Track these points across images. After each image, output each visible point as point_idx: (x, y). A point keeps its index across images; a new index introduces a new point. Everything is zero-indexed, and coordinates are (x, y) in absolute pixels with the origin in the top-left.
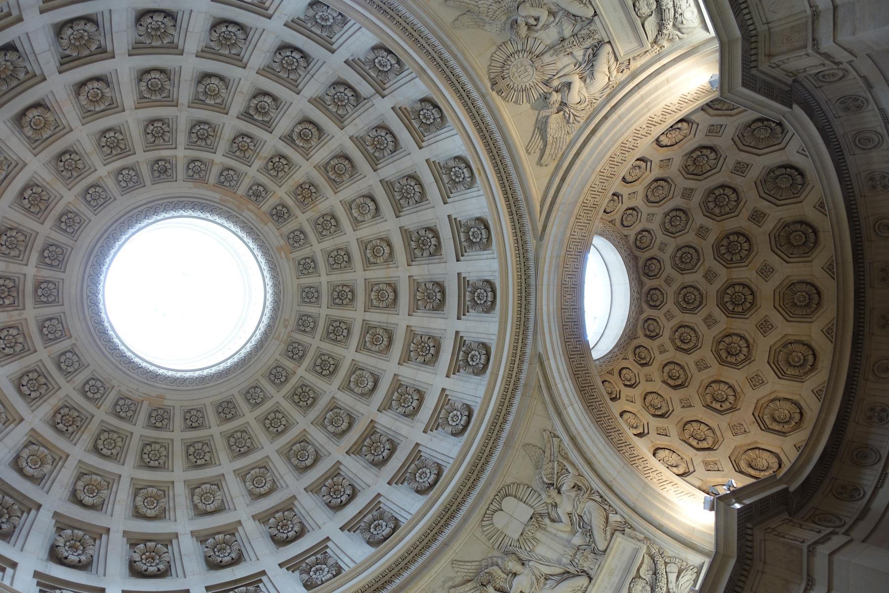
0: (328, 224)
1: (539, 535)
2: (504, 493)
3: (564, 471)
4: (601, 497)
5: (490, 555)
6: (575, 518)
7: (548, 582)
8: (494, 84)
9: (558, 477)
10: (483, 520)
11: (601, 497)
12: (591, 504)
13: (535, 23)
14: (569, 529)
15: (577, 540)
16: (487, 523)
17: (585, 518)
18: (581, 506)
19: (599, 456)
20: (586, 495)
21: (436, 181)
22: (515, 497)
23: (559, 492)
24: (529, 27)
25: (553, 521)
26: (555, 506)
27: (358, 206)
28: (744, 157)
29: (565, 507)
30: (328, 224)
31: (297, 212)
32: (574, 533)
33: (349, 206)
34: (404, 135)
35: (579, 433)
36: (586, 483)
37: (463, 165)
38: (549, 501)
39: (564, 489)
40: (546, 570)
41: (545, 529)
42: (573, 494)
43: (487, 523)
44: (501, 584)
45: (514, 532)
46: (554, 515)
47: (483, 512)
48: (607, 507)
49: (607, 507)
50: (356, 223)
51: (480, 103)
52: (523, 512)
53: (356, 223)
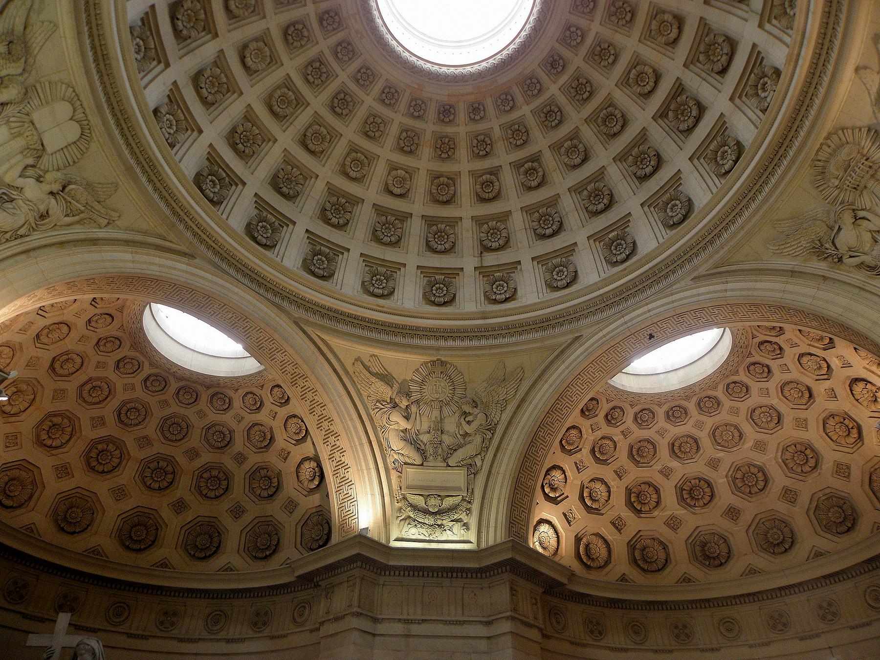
0: (408, 143)
8: (443, 363)
13: (467, 419)
21: (383, 260)
24: (465, 414)
27: (404, 179)
28: (247, 518)
30: (408, 143)
31: (437, 128)
33: (410, 173)
34: (436, 261)
37: (386, 293)
50: (393, 167)
51: (432, 343)
53: (393, 167)
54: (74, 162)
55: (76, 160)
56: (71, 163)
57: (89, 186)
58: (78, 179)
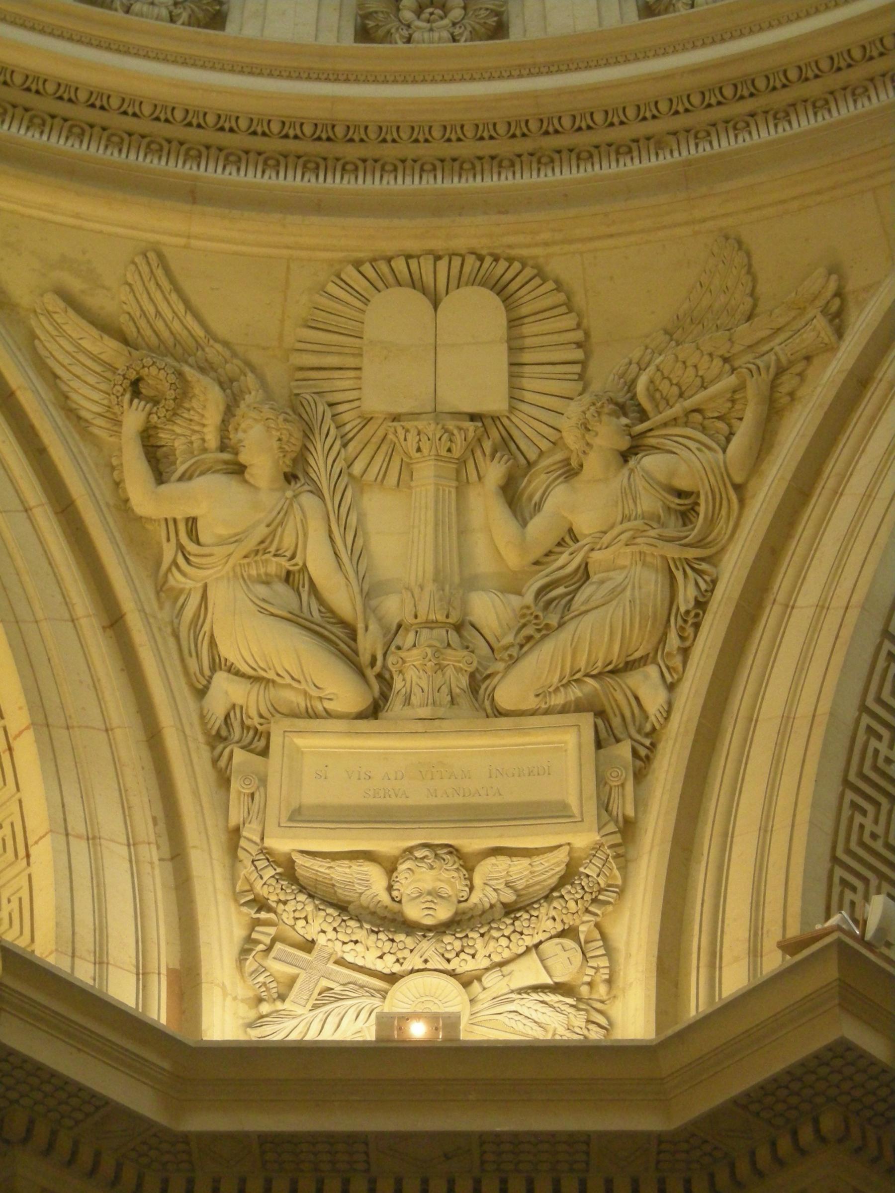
1: (426, 473)
2: (504, 280)
3: (714, 424)
5: (256, 357)
6: (567, 562)
7: (281, 588)
9: (674, 422)
10: (357, 264)
11: (701, 605)
12: (652, 584)
14: (513, 559)
15: (489, 610)
16: (360, 284)
17: (587, 591)
20: (672, 551)
22: (514, 322)
23: (625, 456)
25: (510, 492)
26: (570, 471)
32: (511, 585)
36: (722, 527)
38: (571, 439)
39: (650, 462)
40: (319, 562)
42: (649, 502)
43: (360, 284)
44: (179, 445)
45: (384, 386)
46: (535, 484)
47: (388, 246)
48: (673, 641)
49: (673, 641)
52: (476, 379)
54: (579, 345)
55: (579, 335)
56: (579, 355)
58: (636, 354)
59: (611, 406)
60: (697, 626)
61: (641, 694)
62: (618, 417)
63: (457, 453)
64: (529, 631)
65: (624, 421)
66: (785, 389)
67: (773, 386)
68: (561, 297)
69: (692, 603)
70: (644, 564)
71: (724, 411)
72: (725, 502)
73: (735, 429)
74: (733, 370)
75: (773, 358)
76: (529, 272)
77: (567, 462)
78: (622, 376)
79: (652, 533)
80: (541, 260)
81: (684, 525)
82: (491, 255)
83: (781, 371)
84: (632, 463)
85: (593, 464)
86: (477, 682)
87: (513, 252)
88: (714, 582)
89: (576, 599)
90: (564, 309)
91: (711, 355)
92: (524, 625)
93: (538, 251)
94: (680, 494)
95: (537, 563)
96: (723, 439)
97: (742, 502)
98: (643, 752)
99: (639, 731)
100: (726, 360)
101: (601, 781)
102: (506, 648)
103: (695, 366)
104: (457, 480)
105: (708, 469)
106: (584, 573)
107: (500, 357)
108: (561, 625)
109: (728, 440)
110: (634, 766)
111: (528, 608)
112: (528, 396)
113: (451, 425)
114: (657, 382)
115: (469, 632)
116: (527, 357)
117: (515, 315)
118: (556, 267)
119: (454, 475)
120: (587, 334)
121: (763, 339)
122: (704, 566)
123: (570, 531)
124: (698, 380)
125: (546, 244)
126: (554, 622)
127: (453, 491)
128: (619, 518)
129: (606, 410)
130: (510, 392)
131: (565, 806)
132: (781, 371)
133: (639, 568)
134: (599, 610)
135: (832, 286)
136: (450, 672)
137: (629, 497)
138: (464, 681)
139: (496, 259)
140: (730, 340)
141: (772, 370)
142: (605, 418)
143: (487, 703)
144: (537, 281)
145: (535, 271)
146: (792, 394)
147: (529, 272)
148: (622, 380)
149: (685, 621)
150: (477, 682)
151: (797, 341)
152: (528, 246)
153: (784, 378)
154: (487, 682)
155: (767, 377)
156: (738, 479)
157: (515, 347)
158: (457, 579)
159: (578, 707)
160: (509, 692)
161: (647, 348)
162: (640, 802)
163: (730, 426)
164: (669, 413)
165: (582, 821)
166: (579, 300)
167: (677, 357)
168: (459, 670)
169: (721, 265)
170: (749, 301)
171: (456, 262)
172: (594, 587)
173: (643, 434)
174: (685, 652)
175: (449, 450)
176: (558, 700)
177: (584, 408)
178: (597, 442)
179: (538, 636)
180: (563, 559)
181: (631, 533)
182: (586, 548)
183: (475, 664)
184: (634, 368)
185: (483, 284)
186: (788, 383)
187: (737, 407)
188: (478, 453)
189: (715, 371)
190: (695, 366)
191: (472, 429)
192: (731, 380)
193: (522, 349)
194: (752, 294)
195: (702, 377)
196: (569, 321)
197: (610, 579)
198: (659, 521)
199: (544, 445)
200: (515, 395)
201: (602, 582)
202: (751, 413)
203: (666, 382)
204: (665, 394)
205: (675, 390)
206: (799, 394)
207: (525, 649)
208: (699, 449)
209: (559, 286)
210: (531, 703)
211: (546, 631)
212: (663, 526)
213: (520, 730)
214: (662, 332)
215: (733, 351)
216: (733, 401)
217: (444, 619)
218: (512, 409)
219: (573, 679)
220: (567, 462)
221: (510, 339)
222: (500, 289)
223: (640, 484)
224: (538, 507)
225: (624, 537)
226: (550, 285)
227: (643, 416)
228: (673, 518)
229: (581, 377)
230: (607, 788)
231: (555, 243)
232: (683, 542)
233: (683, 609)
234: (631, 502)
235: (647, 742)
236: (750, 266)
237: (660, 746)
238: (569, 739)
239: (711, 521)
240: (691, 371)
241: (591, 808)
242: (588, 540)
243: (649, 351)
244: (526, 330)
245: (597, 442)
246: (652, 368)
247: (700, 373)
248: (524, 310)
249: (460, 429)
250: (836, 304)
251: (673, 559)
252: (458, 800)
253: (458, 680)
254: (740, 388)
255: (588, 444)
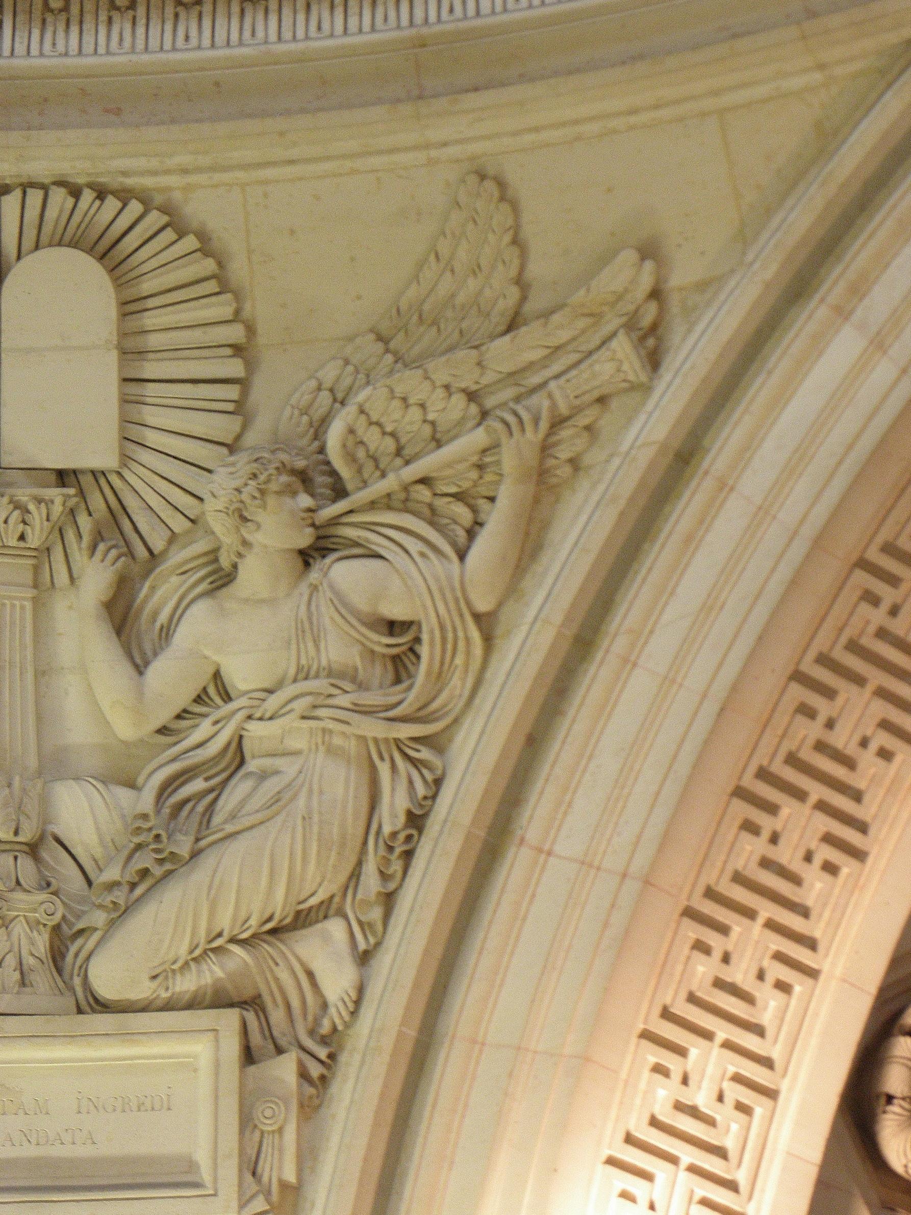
4: (416, 821)
6: (209, 735)
9: (386, 502)
11: (416, 821)
12: (339, 785)
14: (125, 728)
15: (85, 816)
17: (238, 790)
18: (296, 734)
19: (640, 686)
20: (374, 728)
22: (130, 307)
23: (306, 558)
25: (121, 614)
29: (240, 638)
35: (724, 487)
36: (458, 685)
38: (221, 526)
39: (344, 574)
41: (41, 589)
42: (339, 648)
46: (161, 594)
48: (371, 883)
49: (371, 883)
54: (238, 350)
55: (236, 333)
56: (235, 368)
57: (396, 340)
58: (329, 374)
59: (284, 478)
60: (408, 855)
61: (317, 967)
62: (294, 494)
63: (35, 539)
64: (144, 860)
65: (305, 500)
66: (564, 453)
67: (545, 449)
68: (209, 266)
69: (402, 819)
70: (331, 751)
71: (466, 485)
72: (461, 644)
73: (482, 517)
74: (484, 414)
75: (546, 404)
76: (155, 219)
77: (213, 555)
78: (305, 412)
79: (344, 700)
80: (177, 196)
81: (398, 681)
82: (90, 186)
83: (558, 422)
84: (314, 575)
85: (254, 575)
86: (63, 947)
87: (130, 182)
88: (438, 782)
89: (221, 802)
90: (211, 286)
91: (447, 387)
92: (139, 847)
93: (173, 180)
94: (392, 627)
95: (163, 731)
96: (461, 535)
97: (488, 640)
98: (315, 1070)
99: (312, 1033)
100: (472, 396)
101: (246, 1121)
102: (112, 886)
103: (422, 406)
104: (35, 586)
105: (434, 588)
106: (237, 756)
107: (107, 369)
108: (195, 854)
109: (471, 534)
110: (301, 1094)
111: (145, 817)
112: (152, 438)
113: (24, 495)
114: (360, 432)
115: (51, 853)
116: (150, 369)
117: (131, 292)
118: (201, 208)
119: (28, 578)
120: (251, 330)
121: (532, 364)
122: (425, 754)
123: (217, 676)
124: (427, 430)
125: (185, 171)
126: (184, 851)
127: (28, 605)
128: (292, 671)
129: (274, 486)
130: (122, 429)
131: (192, 1165)
132: (558, 422)
133: (321, 755)
134: (254, 832)
135: (646, 281)
136: (19, 929)
137: (308, 635)
138: (42, 942)
139: (101, 194)
140: (479, 364)
141: (544, 425)
142: (271, 500)
143: (77, 981)
144: (169, 235)
145: (165, 219)
146: (574, 462)
147: (155, 219)
148: (305, 419)
149: (391, 849)
150: (63, 947)
151: (585, 376)
152: (154, 173)
153: (565, 433)
154: (80, 941)
155: (533, 437)
156: (482, 606)
157: (130, 350)
158: (32, 762)
159: (219, 1000)
160: (113, 970)
161: (347, 362)
162: (308, 1156)
163: (474, 510)
164: (379, 488)
165: (215, 1195)
166: (238, 269)
167: (392, 391)
168: (34, 925)
169: (470, 226)
170: (514, 293)
171: (35, 198)
172: (248, 785)
173: (335, 521)
174: (389, 900)
175: (22, 538)
176: (186, 985)
177: (238, 483)
178: (258, 538)
179: (158, 871)
180: (205, 728)
181: (308, 700)
182: (240, 716)
183: (58, 917)
184: (325, 398)
185: (74, 244)
186: (570, 441)
187: (489, 477)
188: (70, 535)
189: (456, 415)
190: (422, 406)
191: (58, 501)
192: (478, 437)
193: (141, 353)
194: (520, 281)
195: (433, 423)
196: (222, 308)
197: (277, 772)
198: (353, 680)
199: (179, 524)
200: (129, 440)
201: (263, 776)
202: (509, 497)
203: (375, 430)
204: (372, 448)
205: (389, 444)
206: (587, 460)
207: (139, 891)
208: (422, 555)
209: (206, 248)
210: (143, 991)
211: (173, 866)
212: (362, 686)
213: (127, 1036)
214: (372, 337)
215: (485, 381)
216: (480, 467)
217: (10, 837)
218: (125, 459)
219: (213, 948)
220: (213, 555)
221: (123, 335)
222: (107, 252)
223: (327, 614)
224: (167, 633)
225: (300, 705)
226: (190, 242)
227: (339, 492)
228: (378, 670)
229: (240, 408)
230: (257, 1134)
231: (199, 170)
232: (391, 714)
233: (387, 830)
234: (310, 645)
235: (322, 1053)
236: (517, 228)
237: (343, 1058)
238: (200, 1050)
239: (440, 678)
240: (415, 413)
241: (230, 1171)
242: (243, 702)
243: (350, 368)
244: (150, 320)
245: (258, 538)
246: (351, 410)
247: (431, 417)
248: (147, 286)
249: (39, 501)
250: (651, 311)
251: (376, 740)
252: (29, 1151)
253: (32, 943)
254: (492, 448)
255: (245, 543)
